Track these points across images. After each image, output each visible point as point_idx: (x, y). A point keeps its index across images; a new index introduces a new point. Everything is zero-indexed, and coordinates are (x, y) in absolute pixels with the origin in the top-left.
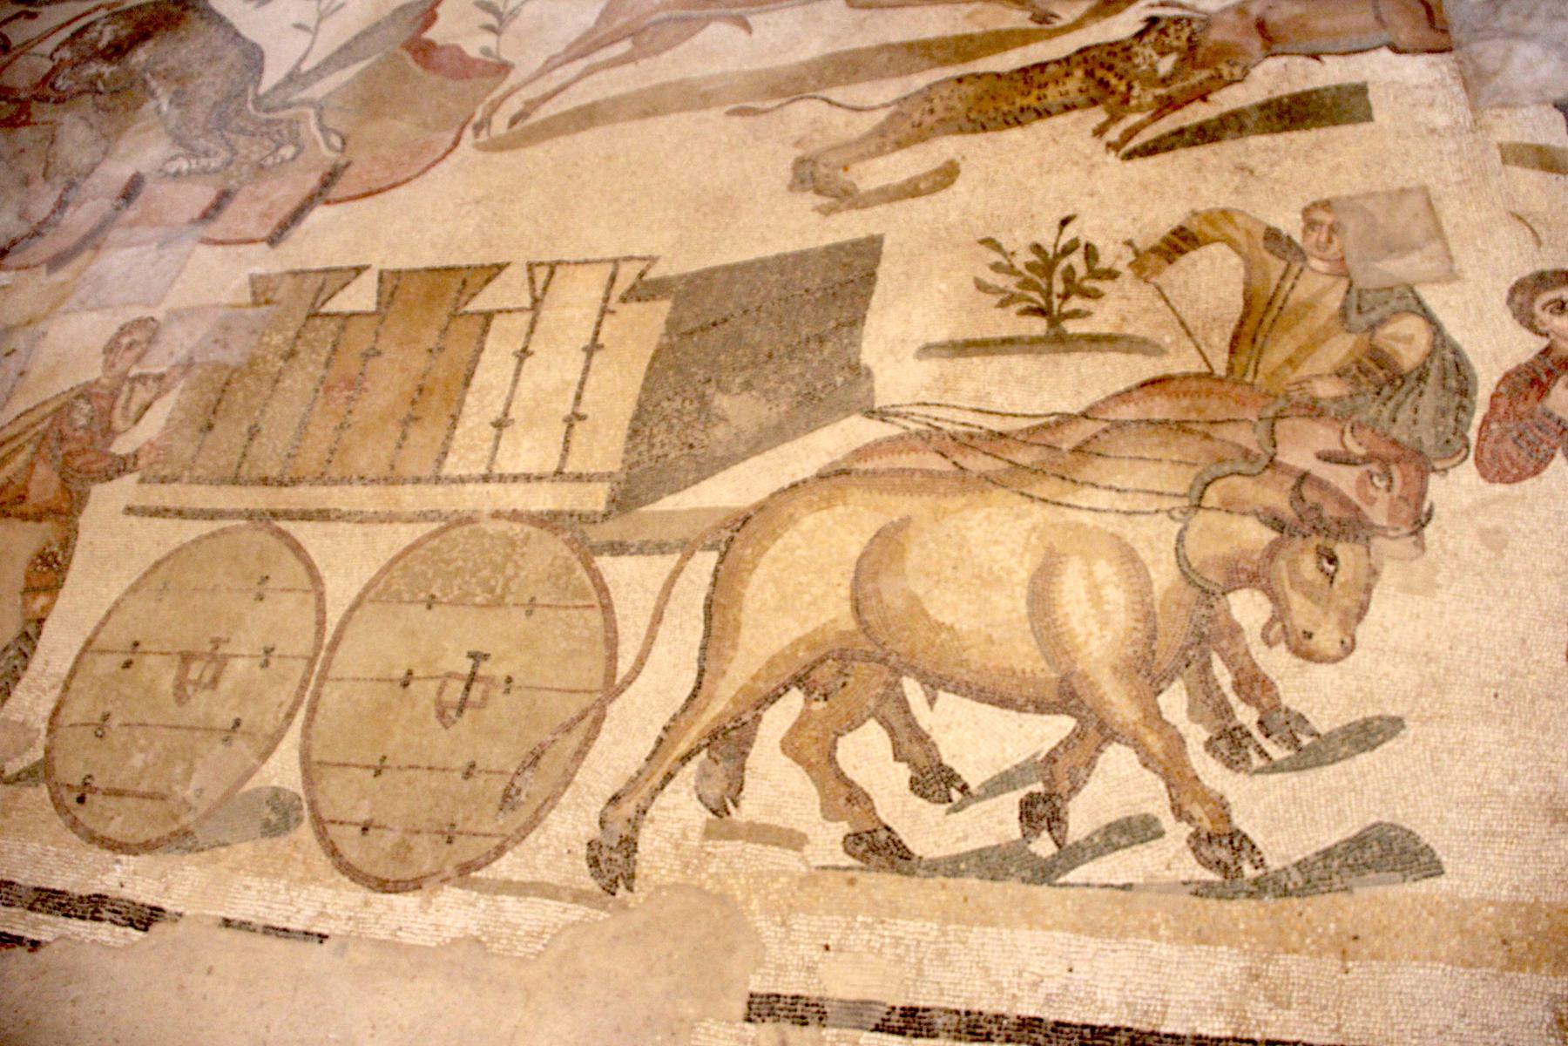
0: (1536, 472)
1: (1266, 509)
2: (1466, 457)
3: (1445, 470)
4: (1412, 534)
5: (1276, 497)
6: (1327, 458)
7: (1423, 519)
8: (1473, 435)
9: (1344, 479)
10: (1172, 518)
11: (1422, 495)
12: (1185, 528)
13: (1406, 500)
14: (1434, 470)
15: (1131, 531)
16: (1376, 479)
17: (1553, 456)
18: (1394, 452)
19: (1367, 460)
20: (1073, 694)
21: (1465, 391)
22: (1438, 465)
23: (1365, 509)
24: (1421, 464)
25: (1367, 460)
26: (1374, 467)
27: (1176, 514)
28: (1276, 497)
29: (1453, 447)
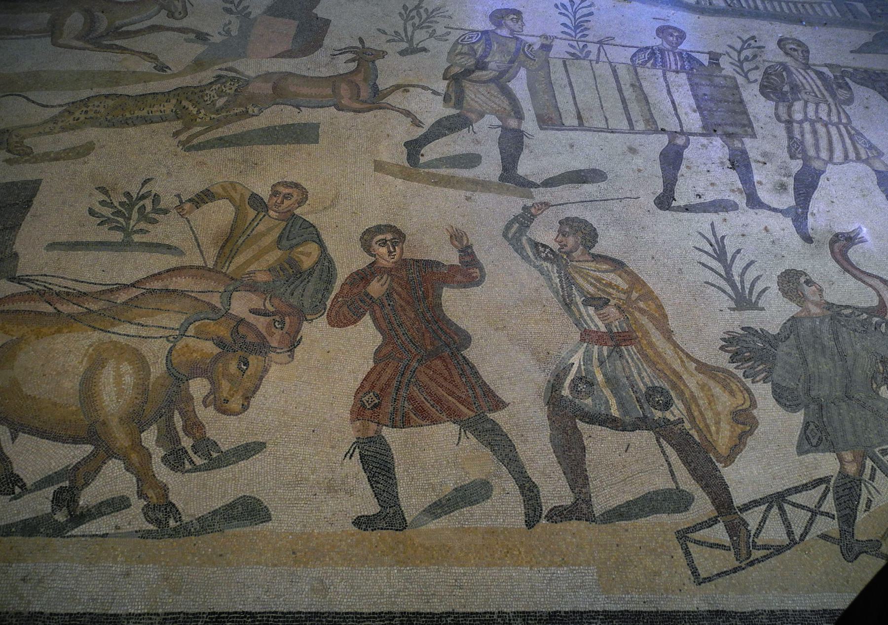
0: (355, 322)
1: (218, 337)
2: (323, 314)
3: (312, 320)
4: (290, 351)
5: (224, 332)
6: (253, 311)
7: (296, 344)
8: (329, 303)
9: (261, 323)
10: (168, 341)
11: (298, 332)
12: (174, 346)
13: (289, 334)
14: (306, 320)
15: (145, 348)
16: (276, 324)
17: (365, 314)
18: (289, 310)
19: (274, 314)
20: (96, 433)
21: (330, 279)
22: (309, 317)
23: (268, 338)
24: (301, 315)
25: (274, 314)
26: (277, 318)
27: (171, 339)
28: (224, 332)
29: (317, 309)
